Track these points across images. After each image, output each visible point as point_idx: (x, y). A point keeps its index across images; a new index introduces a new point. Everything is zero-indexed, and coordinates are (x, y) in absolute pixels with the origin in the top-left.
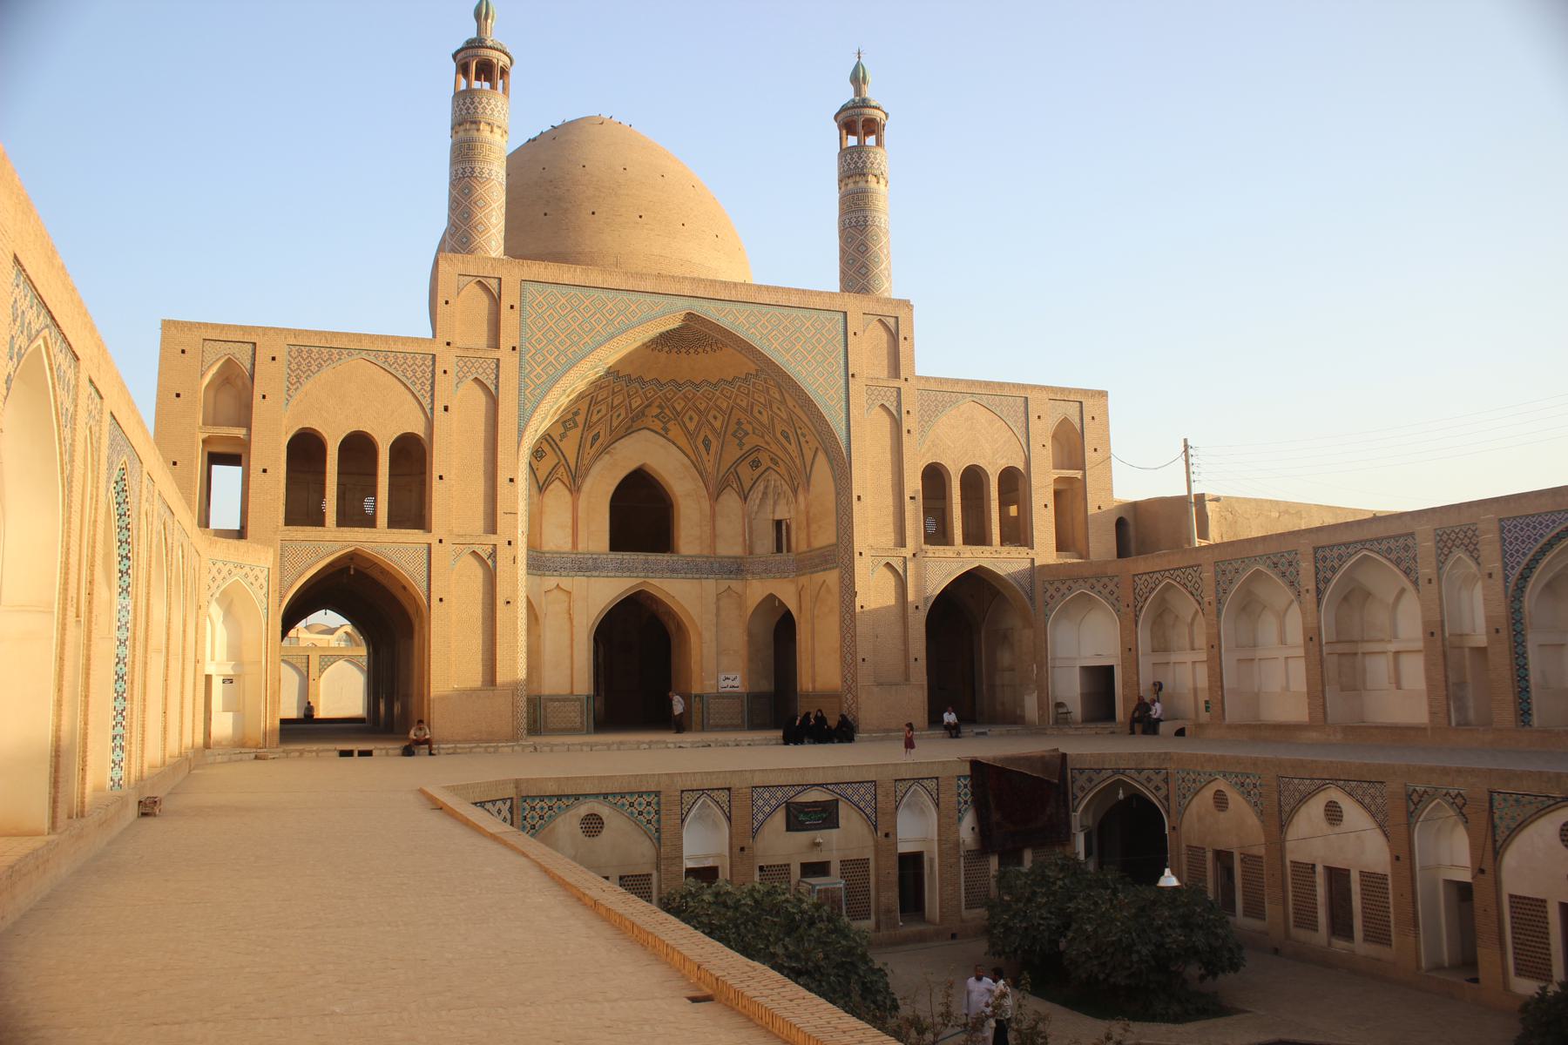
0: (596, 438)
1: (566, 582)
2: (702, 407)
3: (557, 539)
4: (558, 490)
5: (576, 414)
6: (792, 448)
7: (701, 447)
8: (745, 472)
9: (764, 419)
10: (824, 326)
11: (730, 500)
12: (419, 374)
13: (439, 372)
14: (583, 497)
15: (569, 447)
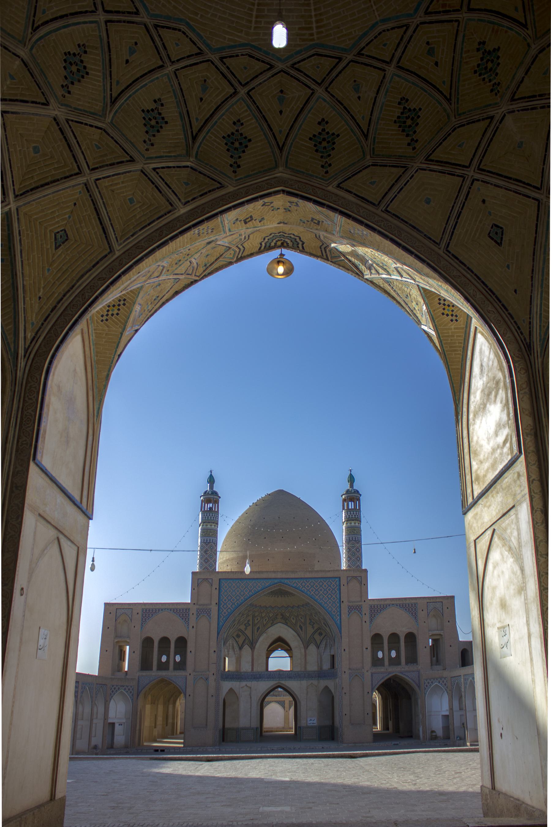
0: (258, 628)
1: (249, 684)
2: (296, 615)
3: (246, 667)
4: (246, 648)
5: (249, 621)
6: (328, 629)
7: (299, 629)
8: (317, 637)
9: (317, 618)
10: (331, 583)
11: (312, 648)
12: (184, 615)
13: (191, 614)
14: (256, 650)
15: (249, 632)
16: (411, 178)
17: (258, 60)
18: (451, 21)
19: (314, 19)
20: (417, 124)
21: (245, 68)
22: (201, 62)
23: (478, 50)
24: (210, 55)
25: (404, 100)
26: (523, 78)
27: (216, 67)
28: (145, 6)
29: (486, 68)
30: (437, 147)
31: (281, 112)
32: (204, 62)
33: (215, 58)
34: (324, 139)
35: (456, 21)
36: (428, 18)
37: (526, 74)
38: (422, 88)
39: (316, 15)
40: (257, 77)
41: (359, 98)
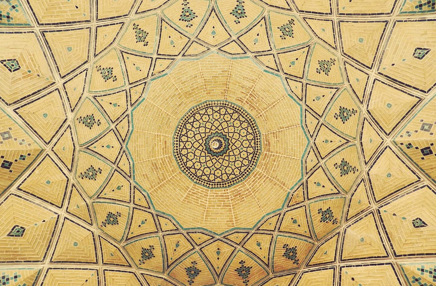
16: (300, 279)
17: (207, 235)
18: (302, 206)
19: (234, 217)
20: (296, 253)
21: (200, 238)
22: (177, 234)
23: (319, 213)
24: (182, 231)
25: (285, 246)
26: (348, 209)
27: (185, 236)
28: (153, 206)
29: (326, 217)
30: (311, 258)
31: (218, 259)
32: (178, 233)
33: (185, 232)
34: (243, 270)
35: (304, 206)
36: (289, 209)
37: (349, 207)
38: (294, 238)
39: (234, 215)
40: (205, 242)
41: (261, 248)
